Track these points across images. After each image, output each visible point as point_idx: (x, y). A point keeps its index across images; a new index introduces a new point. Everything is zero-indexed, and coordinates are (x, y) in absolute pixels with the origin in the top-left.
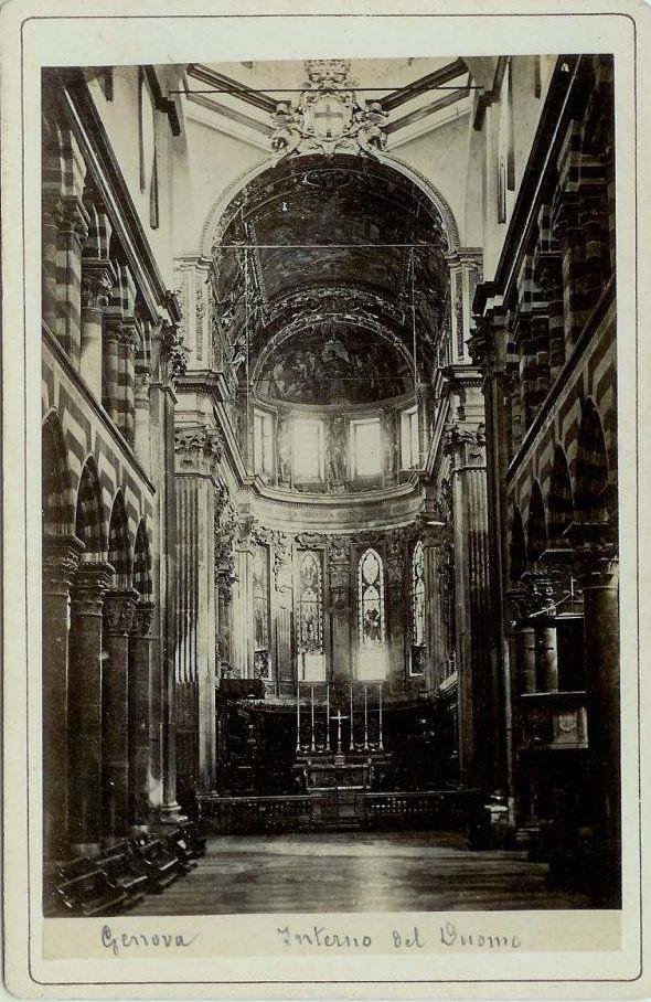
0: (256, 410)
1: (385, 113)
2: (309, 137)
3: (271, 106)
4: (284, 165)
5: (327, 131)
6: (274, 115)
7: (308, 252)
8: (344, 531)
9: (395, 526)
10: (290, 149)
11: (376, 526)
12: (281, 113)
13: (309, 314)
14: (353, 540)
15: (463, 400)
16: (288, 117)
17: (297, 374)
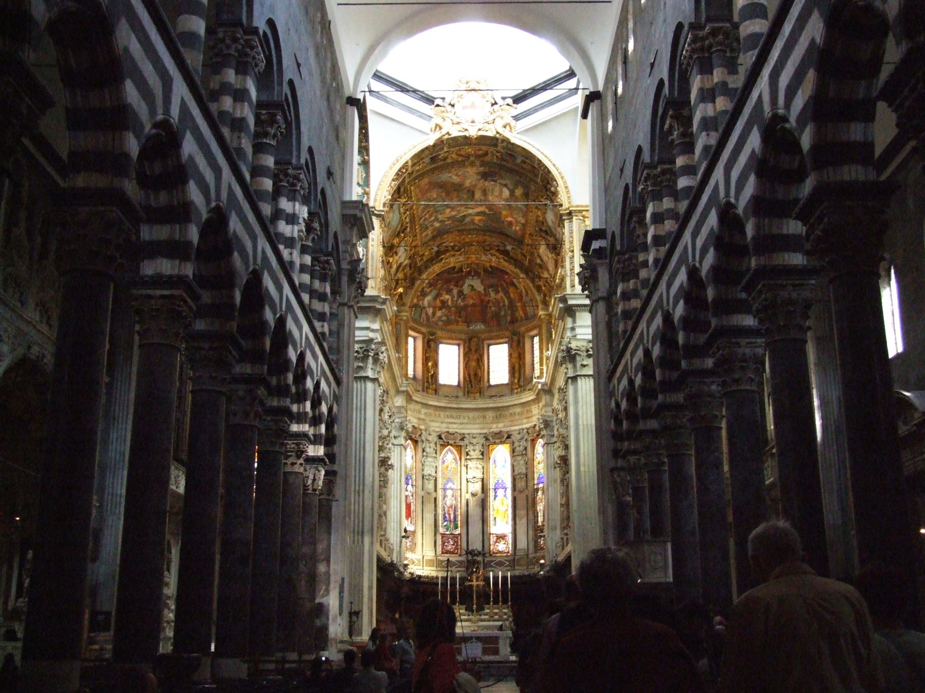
0: (411, 332)
1: (515, 105)
2: (458, 123)
3: (429, 100)
4: (440, 143)
5: (474, 119)
6: (433, 106)
7: (453, 209)
8: (479, 431)
9: (520, 427)
10: (444, 132)
11: (505, 427)
12: (438, 105)
13: (454, 255)
14: (487, 439)
15: (574, 322)
16: (442, 109)
17: (444, 304)
